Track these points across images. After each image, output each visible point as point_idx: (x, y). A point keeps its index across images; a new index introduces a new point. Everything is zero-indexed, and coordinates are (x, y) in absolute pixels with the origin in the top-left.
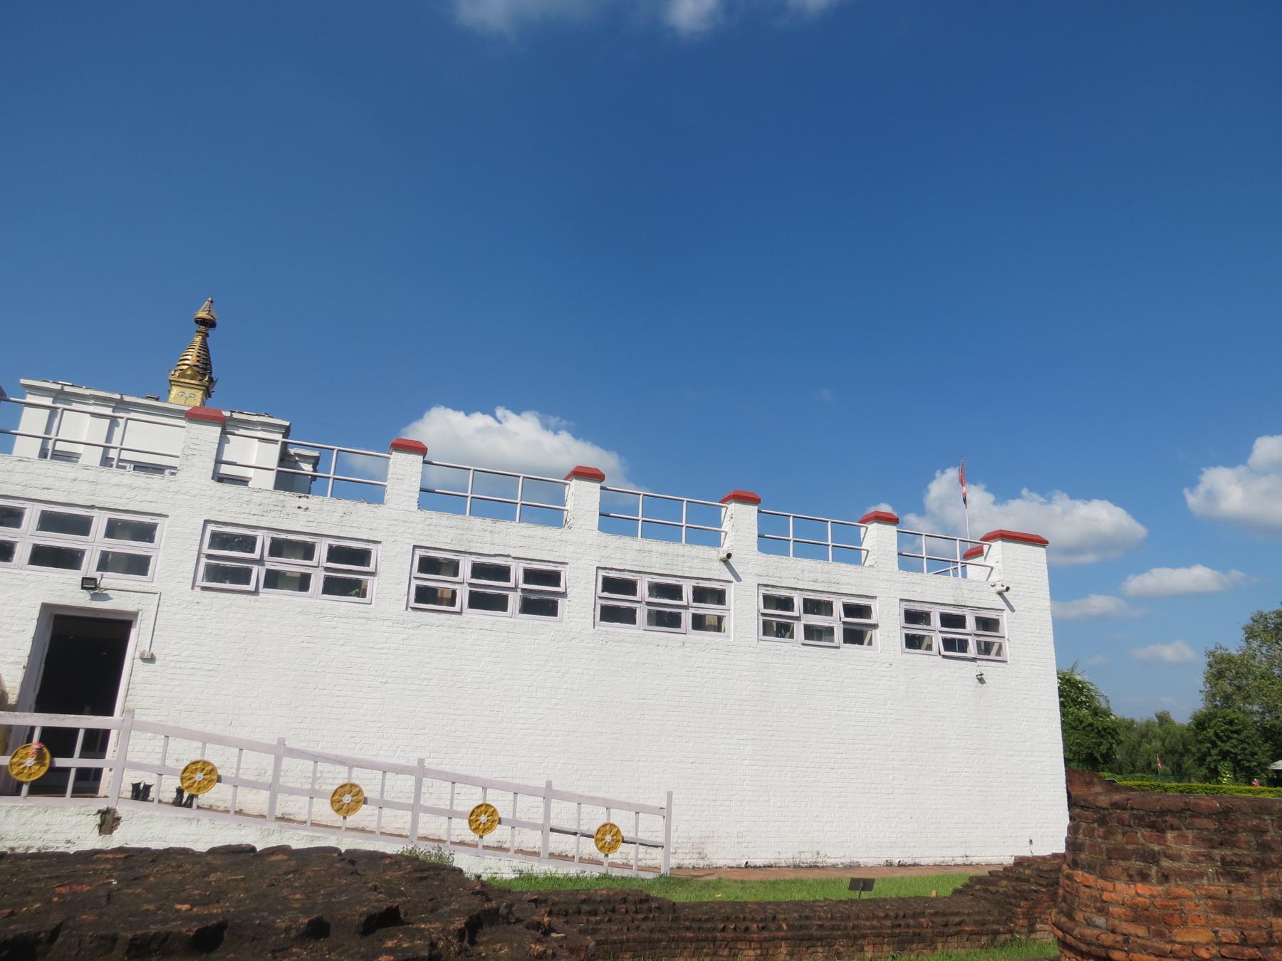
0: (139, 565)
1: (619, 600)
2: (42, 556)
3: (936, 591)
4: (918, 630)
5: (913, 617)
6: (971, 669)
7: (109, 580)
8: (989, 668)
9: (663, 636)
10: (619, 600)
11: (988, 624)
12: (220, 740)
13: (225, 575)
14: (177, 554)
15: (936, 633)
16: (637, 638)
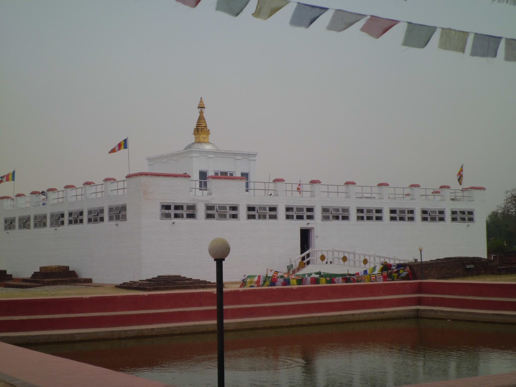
0: (310, 217)
1: (393, 215)
2: (300, 217)
3: (459, 206)
4: (455, 216)
5: (454, 213)
6: (466, 224)
7: (309, 221)
8: (471, 224)
9: (401, 222)
10: (393, 215)
11: (470, 213)
12: (347, 252)
13: (326, 218)
14: (318, 213)
15: (459, 216)
16: (398, 224)
